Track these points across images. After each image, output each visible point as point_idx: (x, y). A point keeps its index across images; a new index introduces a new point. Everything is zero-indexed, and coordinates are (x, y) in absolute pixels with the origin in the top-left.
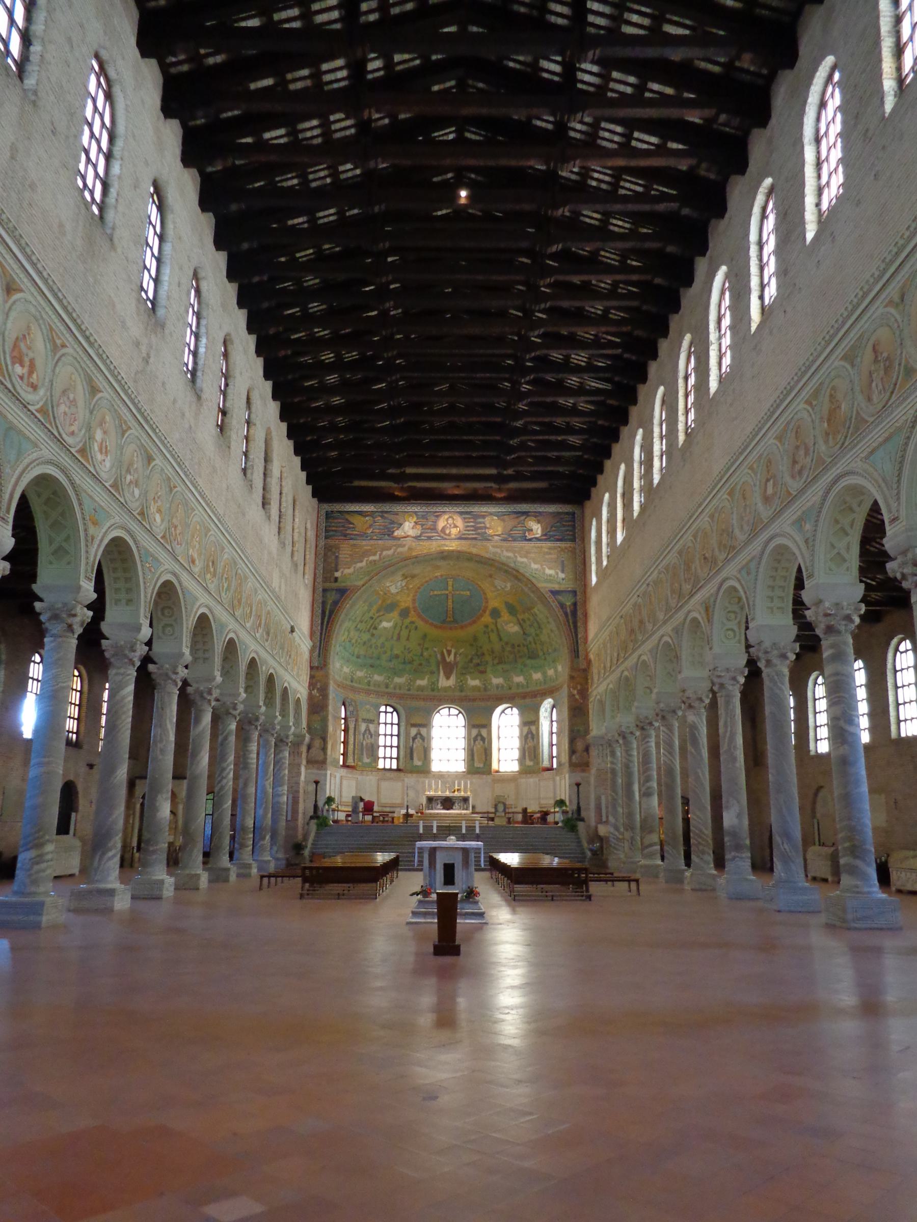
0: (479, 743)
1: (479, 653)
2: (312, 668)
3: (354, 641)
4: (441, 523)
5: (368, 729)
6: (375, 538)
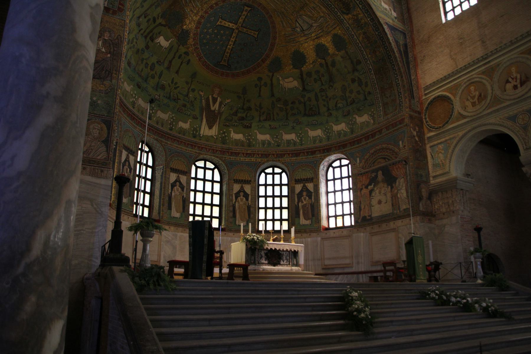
0: (242, 199)
5: (127, 160)
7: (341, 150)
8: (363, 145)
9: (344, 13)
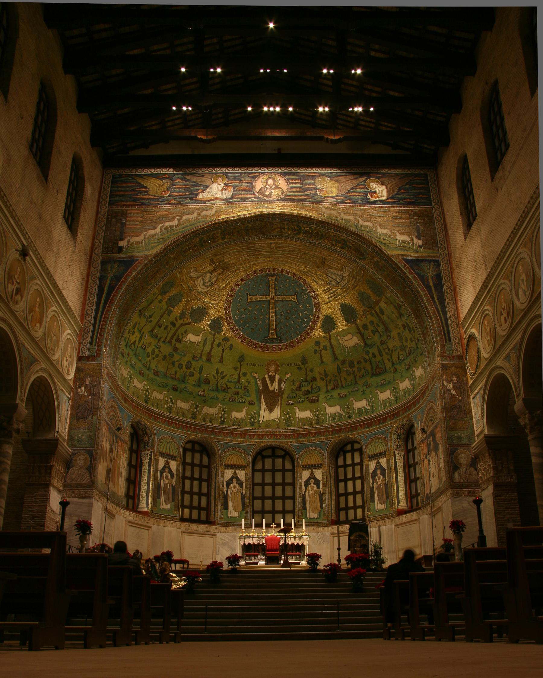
0: (312, 486)
1: (308, 379)
2: (79, 359)
3: (149, 350)
4: (259, 185)
5: (167, 466)
6: (174, 202)
7: (407, 413)
8: (421, 405)
9: (360, 259)
